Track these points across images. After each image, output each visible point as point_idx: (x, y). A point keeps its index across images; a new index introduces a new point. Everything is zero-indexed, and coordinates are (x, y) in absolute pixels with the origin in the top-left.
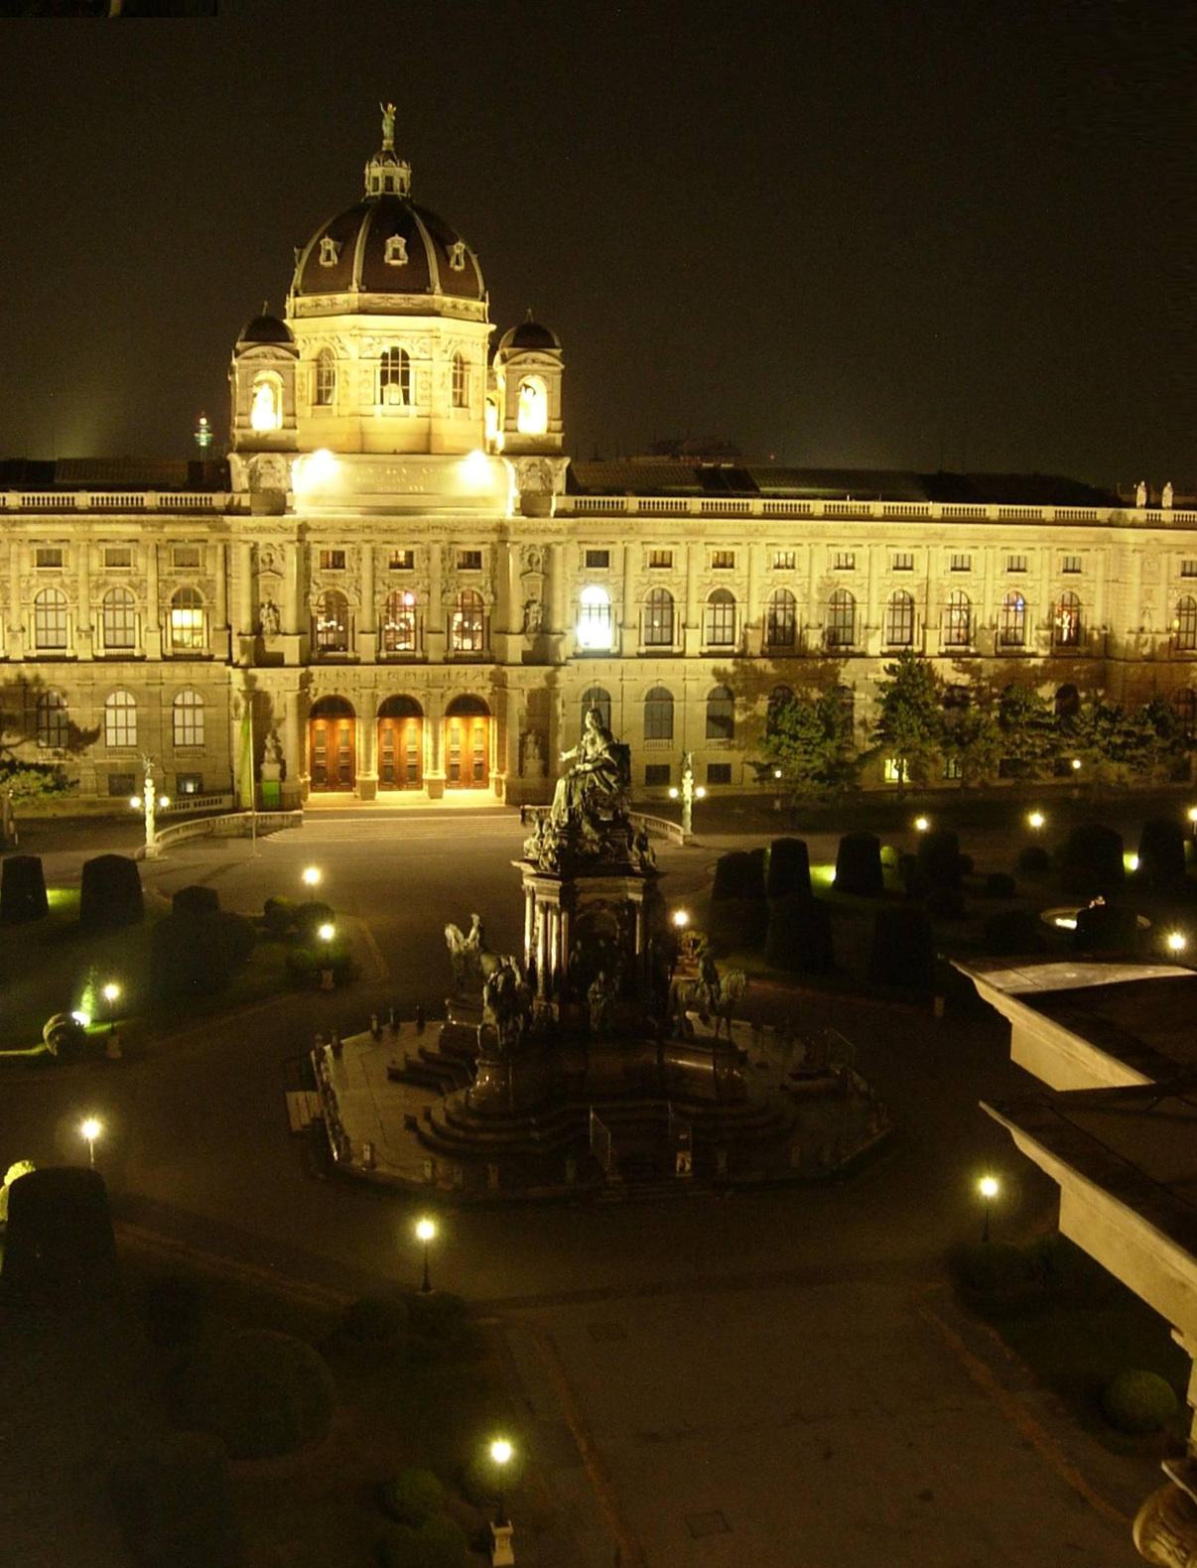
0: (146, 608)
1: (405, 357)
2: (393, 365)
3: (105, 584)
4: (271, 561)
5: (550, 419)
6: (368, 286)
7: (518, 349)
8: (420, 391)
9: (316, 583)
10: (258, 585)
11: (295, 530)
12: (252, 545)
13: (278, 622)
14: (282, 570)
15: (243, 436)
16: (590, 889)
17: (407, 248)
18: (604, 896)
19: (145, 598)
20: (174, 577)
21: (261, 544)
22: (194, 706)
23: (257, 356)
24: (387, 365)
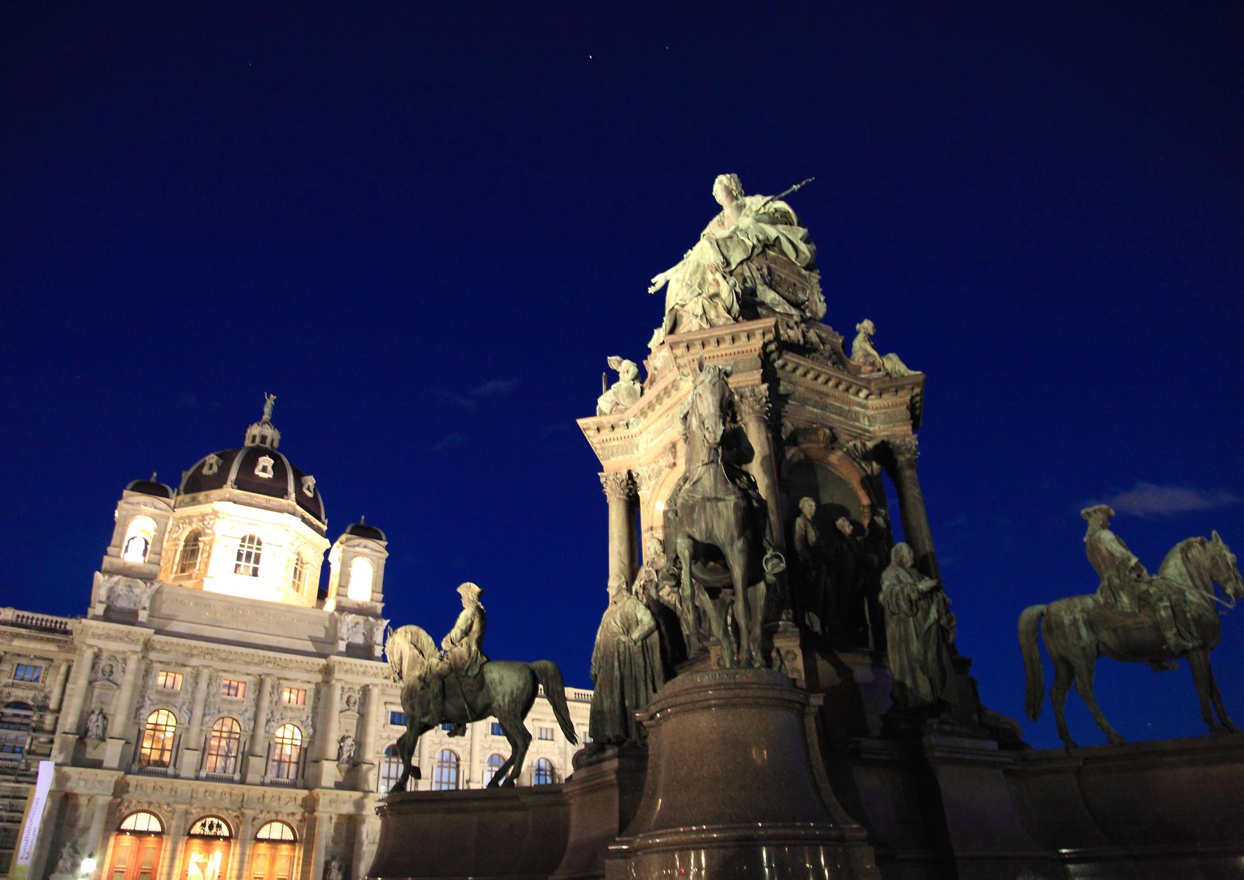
1: (259, 543)
2: (248, 547)
4: (111, 672)
5: (373, 591)
6: (240, 484)
7: (353, 536)
9: (149, 699)
10: (92, 693)
11: (141, 643)
12: (96, 650)
13: (105, 729)
14: (119, 682)
15: (111, 563)
17: (273, 467)
21: (105, 655)
23: (138, 504)
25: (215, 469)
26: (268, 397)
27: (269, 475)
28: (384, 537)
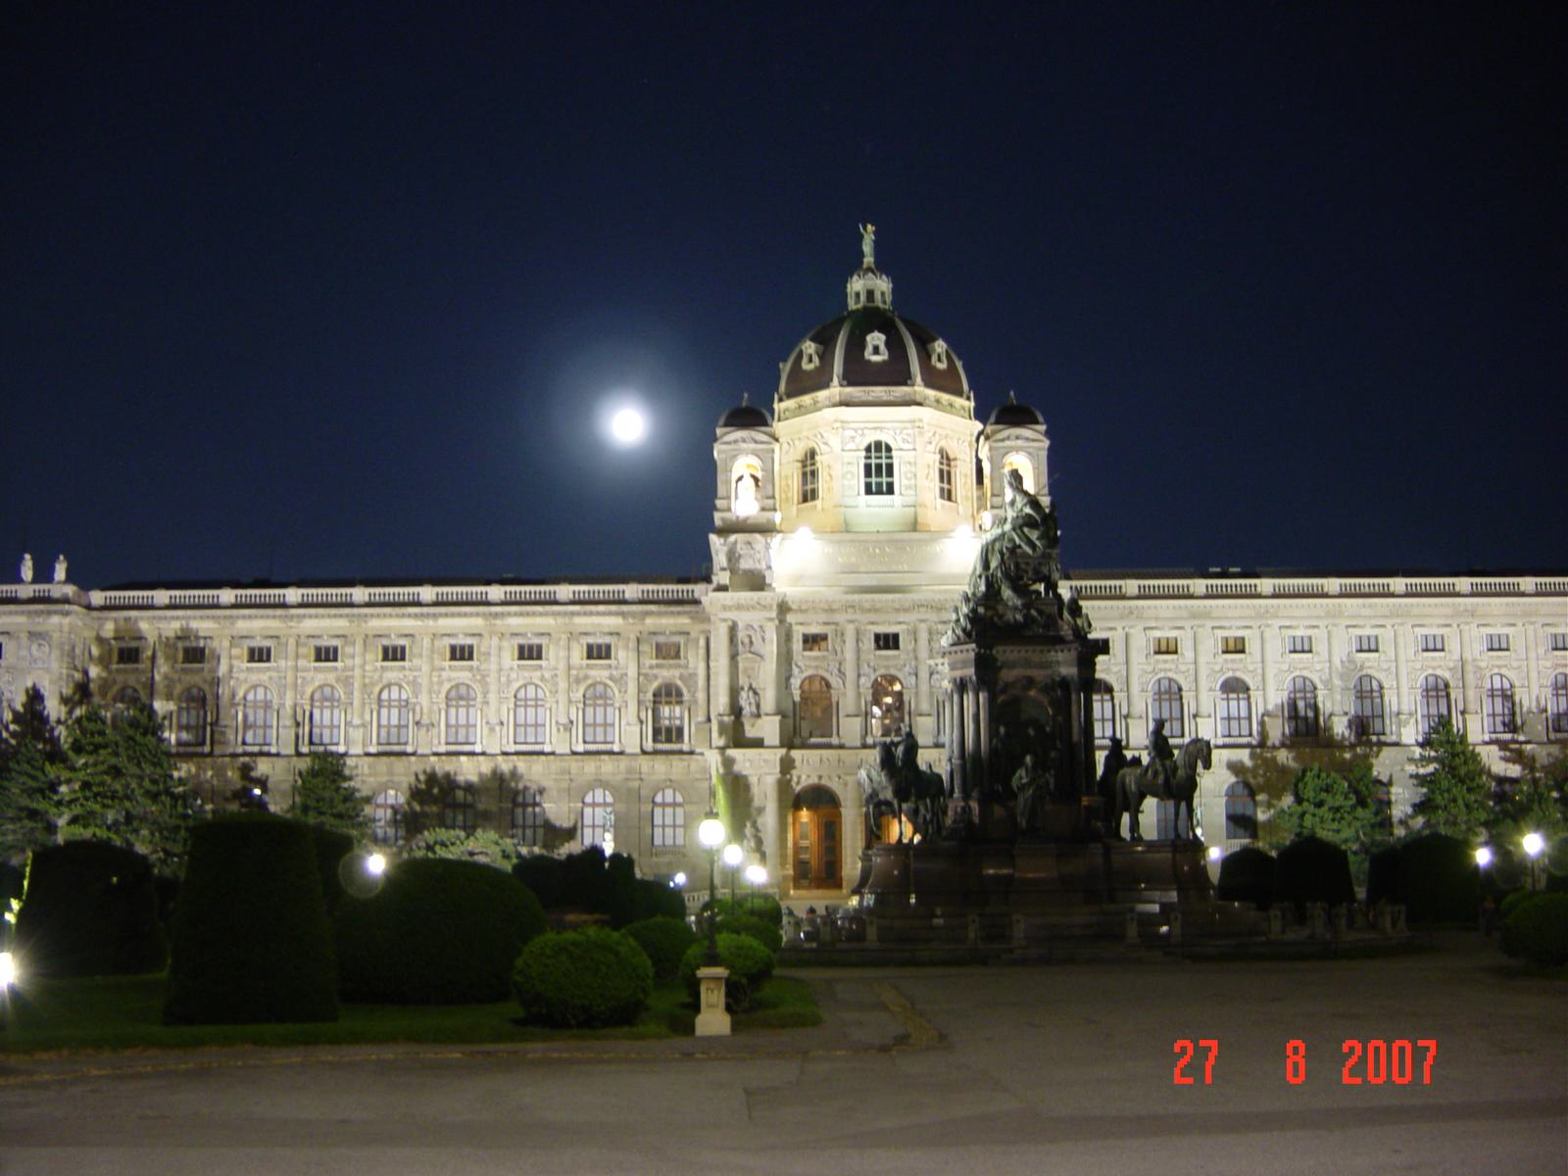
0: (626, 702)
1: (889, 449)
2: (877, 458)
3: (586, 677)
4: (751, 643)
6: (851, 378)
7: (1001, 427)
8: (905, 482)
9: (796, 665)
10: (737, 667)
11: (775, 607)
12: (730, 623)
13: (758, 706)
14: (762, 652)
15: (723, 519)
16: (1012, 666)
17: (887, 344)
18: (1030, 672)
19: (626, 692)
20: (655, 671)
21: (741, 625)
22: (674, 805)
23: (736, 442)
24: (870, 458)
25: (816, 359)
26: (865, 228)
27: (882, 357)
28: (1041, 419)
